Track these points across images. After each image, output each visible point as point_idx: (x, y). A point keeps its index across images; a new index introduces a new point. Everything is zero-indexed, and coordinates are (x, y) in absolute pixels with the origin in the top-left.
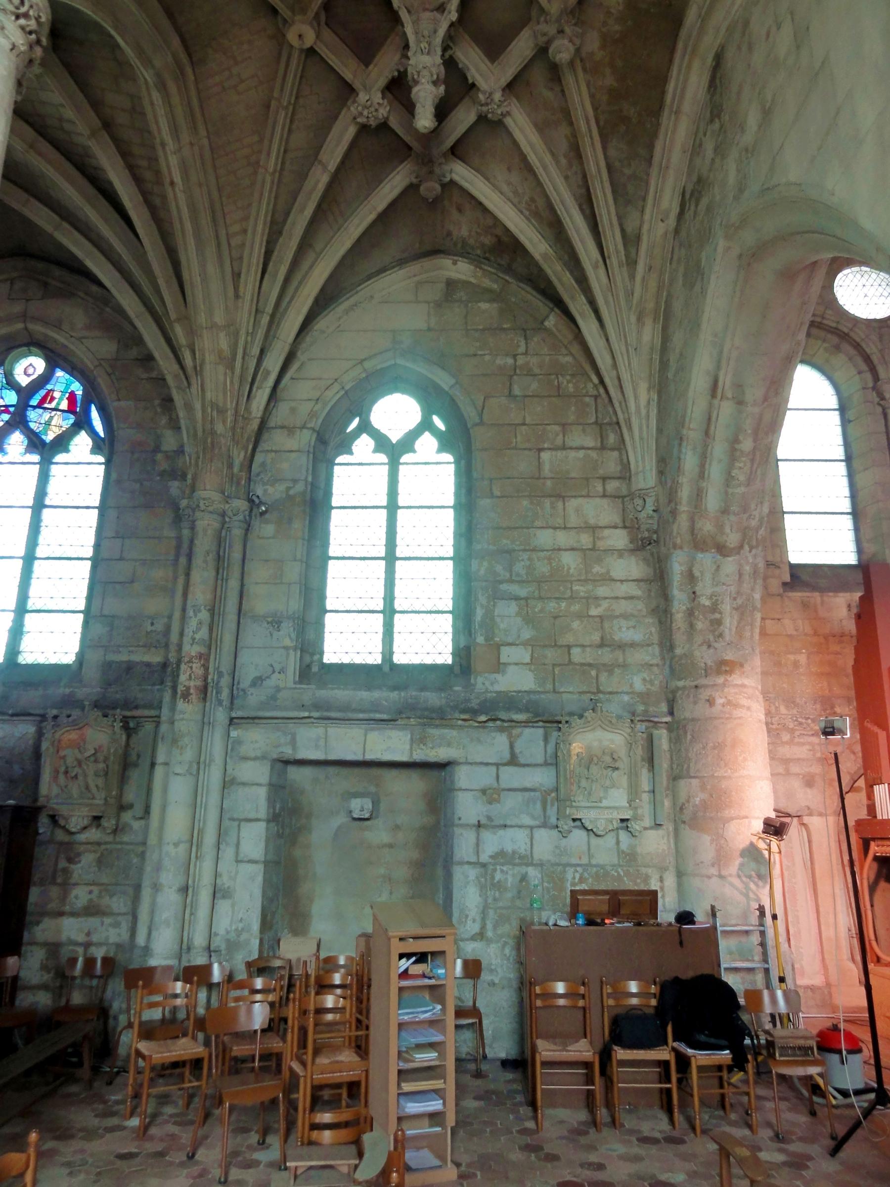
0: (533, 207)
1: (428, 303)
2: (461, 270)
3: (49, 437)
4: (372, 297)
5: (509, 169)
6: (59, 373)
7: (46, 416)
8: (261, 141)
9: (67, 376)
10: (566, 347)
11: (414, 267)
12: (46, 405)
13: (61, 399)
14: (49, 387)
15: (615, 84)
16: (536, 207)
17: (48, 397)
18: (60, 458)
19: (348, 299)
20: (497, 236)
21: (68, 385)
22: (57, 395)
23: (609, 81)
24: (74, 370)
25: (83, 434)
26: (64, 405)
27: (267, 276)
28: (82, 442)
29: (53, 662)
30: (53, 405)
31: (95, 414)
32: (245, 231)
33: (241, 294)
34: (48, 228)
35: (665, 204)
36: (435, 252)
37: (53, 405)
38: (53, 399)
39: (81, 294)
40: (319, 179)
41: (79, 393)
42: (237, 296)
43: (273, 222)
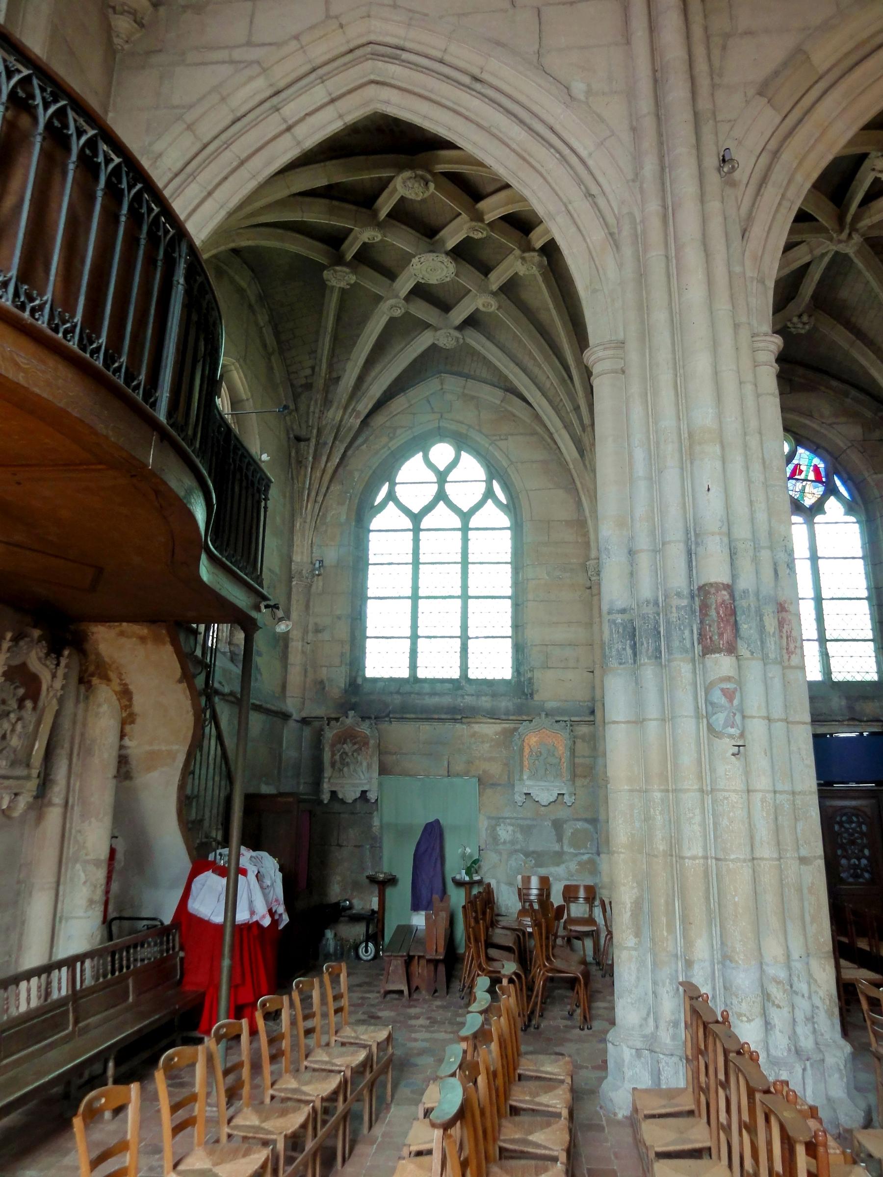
3: (808, 502)
6: (800, 450)
7: (799, 485)
9: (808, 453)
12: (796, 477)
13: (808, 472)
14: (795, 462)
17: (796, 470)
18: (818, 518)
21: (811, 460)
22: (802, 468)
24: (815, 449)
25: (832, 498)
26: (812, 476)
28: (833, 505)
29: (859, 679)
30: (802, 476)
31: (838, 483)
34: (845, 345)
37: (802, 476)
38: (801, 472)
39: (823, 388)
41: (821, 466)
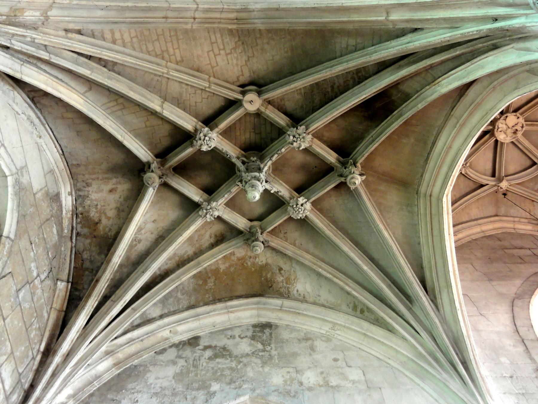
0: (135, 243)
1: (46, 186)
2: (67, 202)
4: (40, 137)
5: (154, 221)
8: (177, 63)
10: (51, 308)
11: (62, 165)
15: (221, 271)
16: (136, 245)
19: (38, 118)
20: (100, 220)
23: (222, 267)
27: (75, 56)
32: (114, 42)
33: (70, 35)
35: (181, 328)
36: (73, 176)
40: (155, 104)
42: (66, 30)
43: (115, 64)
